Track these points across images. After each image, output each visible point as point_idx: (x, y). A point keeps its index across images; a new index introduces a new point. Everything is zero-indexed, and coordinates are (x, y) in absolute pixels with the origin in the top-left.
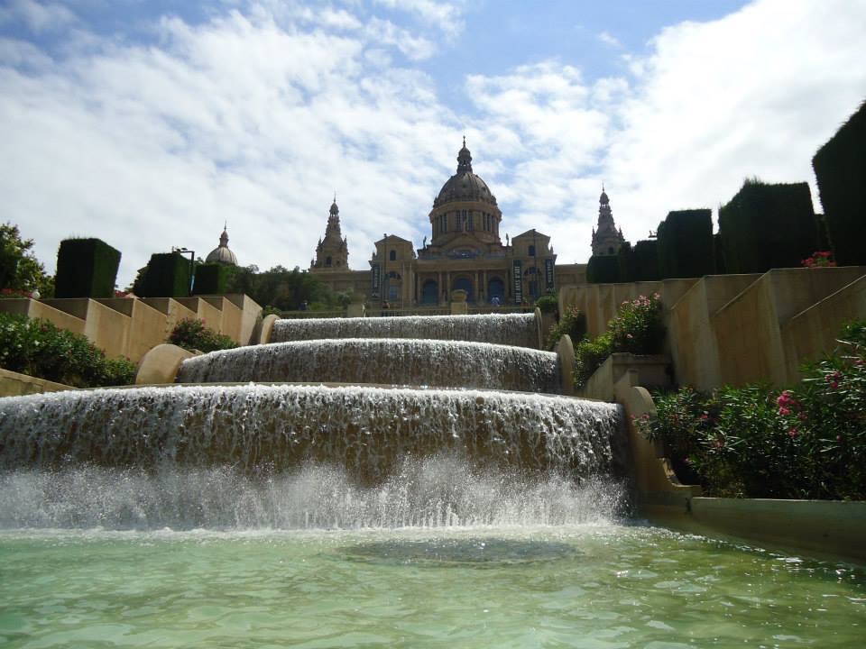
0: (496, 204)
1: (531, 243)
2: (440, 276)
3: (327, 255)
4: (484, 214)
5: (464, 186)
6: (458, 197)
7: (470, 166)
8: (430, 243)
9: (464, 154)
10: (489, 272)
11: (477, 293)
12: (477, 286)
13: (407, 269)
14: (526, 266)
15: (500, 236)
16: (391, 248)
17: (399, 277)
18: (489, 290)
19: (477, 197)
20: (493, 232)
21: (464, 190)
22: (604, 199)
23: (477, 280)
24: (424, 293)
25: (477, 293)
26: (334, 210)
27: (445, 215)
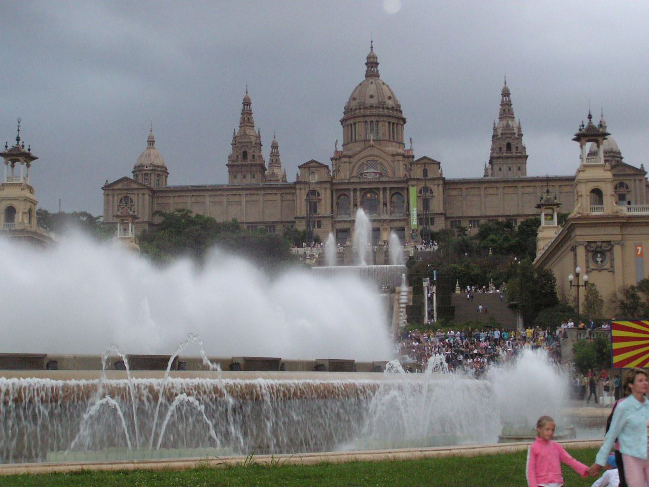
0: (401, 112)
3: (243, 150)
4: (389, 123)
5: (372, 97)
7: (378, 71)
9: (372, 60)
10: (391, 189)
12: (381, 201)
13: (326, 189)
14: (422, 185)
17: (319, 195)
18: (391, 202)
23: (381, 196)
25: (381, 205)
26: (247, 103)
27: (355, 124)
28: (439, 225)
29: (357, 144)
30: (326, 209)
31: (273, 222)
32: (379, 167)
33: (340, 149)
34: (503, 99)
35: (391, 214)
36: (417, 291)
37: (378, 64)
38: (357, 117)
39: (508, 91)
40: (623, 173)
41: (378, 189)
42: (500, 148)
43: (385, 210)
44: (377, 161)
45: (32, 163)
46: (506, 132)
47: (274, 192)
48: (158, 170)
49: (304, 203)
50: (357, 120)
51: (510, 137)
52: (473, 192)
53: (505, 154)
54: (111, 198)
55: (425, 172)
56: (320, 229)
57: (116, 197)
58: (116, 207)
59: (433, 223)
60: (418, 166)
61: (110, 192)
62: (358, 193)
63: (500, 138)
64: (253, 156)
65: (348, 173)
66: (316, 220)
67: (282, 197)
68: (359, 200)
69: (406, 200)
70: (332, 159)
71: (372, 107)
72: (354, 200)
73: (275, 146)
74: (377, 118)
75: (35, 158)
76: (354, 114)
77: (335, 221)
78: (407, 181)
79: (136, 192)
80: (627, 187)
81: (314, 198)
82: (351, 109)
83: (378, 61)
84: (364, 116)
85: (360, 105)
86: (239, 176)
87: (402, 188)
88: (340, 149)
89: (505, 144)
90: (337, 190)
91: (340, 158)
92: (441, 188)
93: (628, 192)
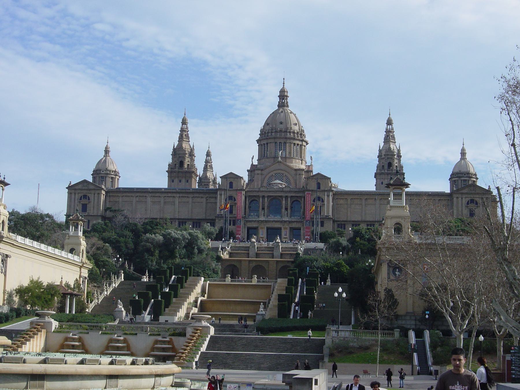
2: (261, 199)
5: (281, 123)
6: (276, 132)
7: (287, 102)
11: (283, 210)
12: (284, 206)
17: (235, 200)
18: (291, 208)
19: (290, 132)
20: (301, 157)
21: (282, 126)
22: (389, 122)
23: (284, 202)
24: (250, 207)
25: (283, 210)
27: (267, 144)
28: (329, 227)
29: (267, 160)
31: (199, 219)
32: (284, 178)
33: (256, 163)
34: (387, 127)
35: (291, 217)
36: (292, 284)
37: (287, 96)
38: (270, 138)
39: (391, 120)
40: (474, 192)
41: (281, 197)
43: (286, 214)
44: (283, 174)
45: (6, 188)
46: (388, 153)
47: (201, 195)
48: (112, 175)
50: (269, 141)
51: (391, 158)
53: (386, 171)
54: (73, 196)
55: (319, 185)
56: (234, 227)
57: (77, 195)
58: (76, 202)
59: (322, 225)
61: (73, 191)
62: (266, 199)
63: (383, 158)
64: (188, 165)
65: (260, 182)
66: (232, 219)
67: (207, 200)
68: (266, 205)
69: (303, 207)
70: (248, 171)
71: (281, 131)
72: (262, 204)
73: (208, 154)
74: (285, 140)
75: (8, 184)
76: (268, 136)
77: (247, 221)
78: (303, 192)
79: (93, 192)
80: (477, 203)
82: (265, 132)
83: (288, 95)
84: (275, 138)
85: (272, 130)
86: (176, 180)
87: (300, 197)
88: (256, 163)
89: (387, 163)
91: (254, 170)
93: (477, 207)
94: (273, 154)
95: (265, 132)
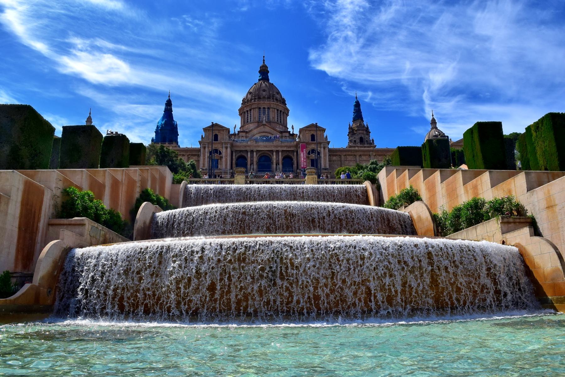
1: (312, 132)
2: (249, 154)
4: (278, 110)
8: (239, 130)
11: (274, 166)
12: (275, 161)
13: (226, 148)
15: (288, 127)
16: (214, 131)
17: (220, 153)
19: (273, 99)
21: (264, 93)
23: (275, 157)
25: (274, 166)
27: (250, 110)
29: (251, 125)
30: (226, 165)
42: (355, 141)
49: (207, 160)
51: (363, 133)
52: (349, 158)
60: (307, 132)
62: (255, 153)
71: (264, 97)
81: (216, 156)
82: (248, 100)
87: (293, 151)
90: (236, 151)
92: (327, 150)
94: (257, 119)
95: (248, 100)
